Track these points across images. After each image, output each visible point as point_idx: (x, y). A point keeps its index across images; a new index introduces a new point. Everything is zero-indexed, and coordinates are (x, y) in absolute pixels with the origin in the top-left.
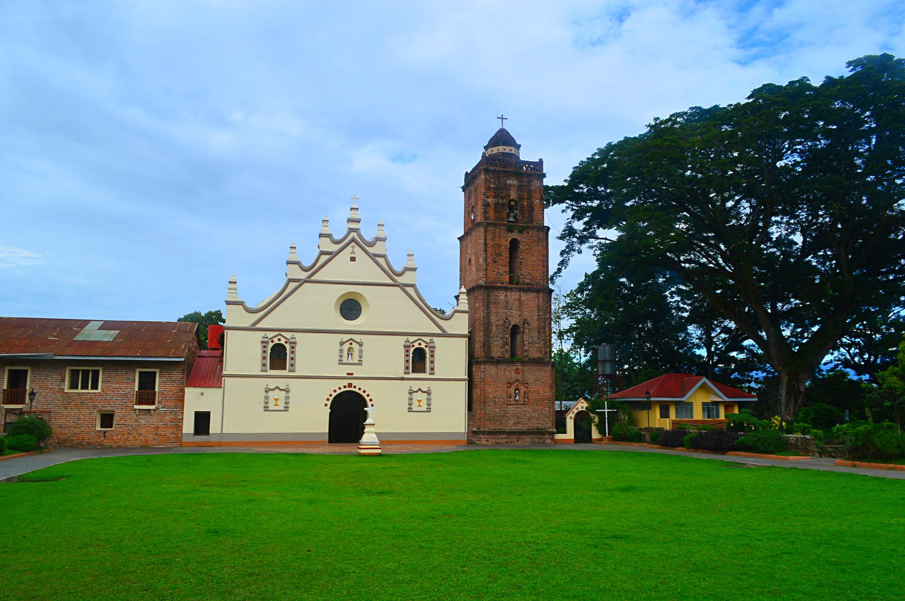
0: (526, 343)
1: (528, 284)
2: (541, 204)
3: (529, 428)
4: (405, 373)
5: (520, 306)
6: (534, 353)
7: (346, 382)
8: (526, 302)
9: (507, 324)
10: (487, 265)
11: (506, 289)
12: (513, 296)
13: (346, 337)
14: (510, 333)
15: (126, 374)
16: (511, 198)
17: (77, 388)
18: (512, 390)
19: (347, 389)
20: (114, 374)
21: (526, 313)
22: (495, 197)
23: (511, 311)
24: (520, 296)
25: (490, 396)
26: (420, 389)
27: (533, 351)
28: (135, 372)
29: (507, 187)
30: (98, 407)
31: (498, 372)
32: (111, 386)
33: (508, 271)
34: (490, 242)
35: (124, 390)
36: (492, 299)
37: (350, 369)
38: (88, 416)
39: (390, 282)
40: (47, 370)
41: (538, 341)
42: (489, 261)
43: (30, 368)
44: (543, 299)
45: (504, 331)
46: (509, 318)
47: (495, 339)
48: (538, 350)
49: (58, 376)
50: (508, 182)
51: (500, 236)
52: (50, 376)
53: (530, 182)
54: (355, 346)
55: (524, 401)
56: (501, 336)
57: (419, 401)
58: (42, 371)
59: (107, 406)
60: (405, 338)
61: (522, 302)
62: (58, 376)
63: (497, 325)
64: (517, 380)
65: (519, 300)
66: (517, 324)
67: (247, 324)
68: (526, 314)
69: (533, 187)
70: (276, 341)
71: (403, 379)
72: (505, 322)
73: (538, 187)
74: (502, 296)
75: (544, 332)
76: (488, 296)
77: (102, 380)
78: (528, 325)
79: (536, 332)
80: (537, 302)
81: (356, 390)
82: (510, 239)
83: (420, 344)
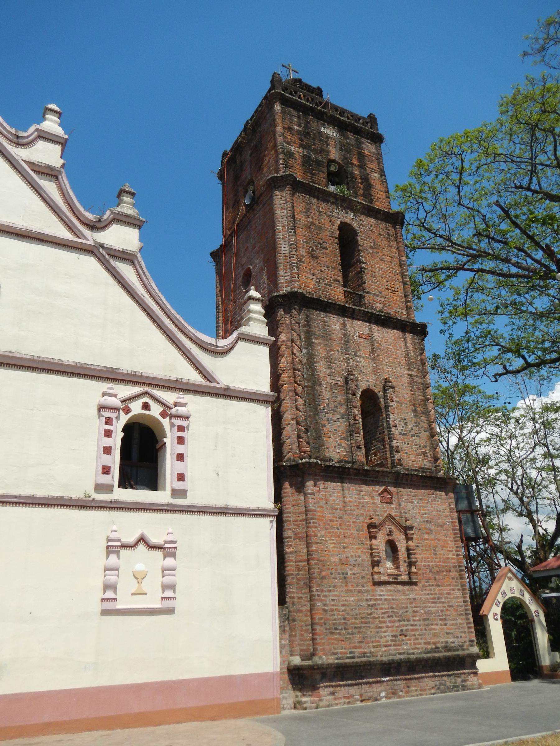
0: (395, 432)
2: (382, 181)
3: (429, 647)
4: (99, 488)
5: (373, 351)
6: (412, 458)
8: (383, 346)
9: (352, 384)
10: (300, 260)
14: (359, 406)
16: (332, 156)
18: (380, 543)
21: (385, 367)
22: (301, 146)
23: (357, 358)
24: (370, 330)
25: (333, 559)
26: (142, 539)
27: (410, 453)
31: (344, 497)
33: (340, 279)
34: (301, 218)
41: (415, 431)
44: (414, 344)
45: (348, 400)
46: (354, 372)
47: (329, 415)
48: (419, 451)
50: (322, 129)
51: (320, 212)
53: (359, 145)
55: (410, 574)
56: (342, 411)
57: (139, 577)
60: (105, 386)
61: (376, 344)
63: (331, 384)
64: (390, 517)
65: (369, 338)
66: (373, 388)
68: (387, 371)
69: (366, 152)
72: (347, 381)
73: (373, 153)
75: (426, 413)
78: (394, 392)
79: (410, 409)
80: (403, 348)
82: (339, 222)
83: (146, 406)
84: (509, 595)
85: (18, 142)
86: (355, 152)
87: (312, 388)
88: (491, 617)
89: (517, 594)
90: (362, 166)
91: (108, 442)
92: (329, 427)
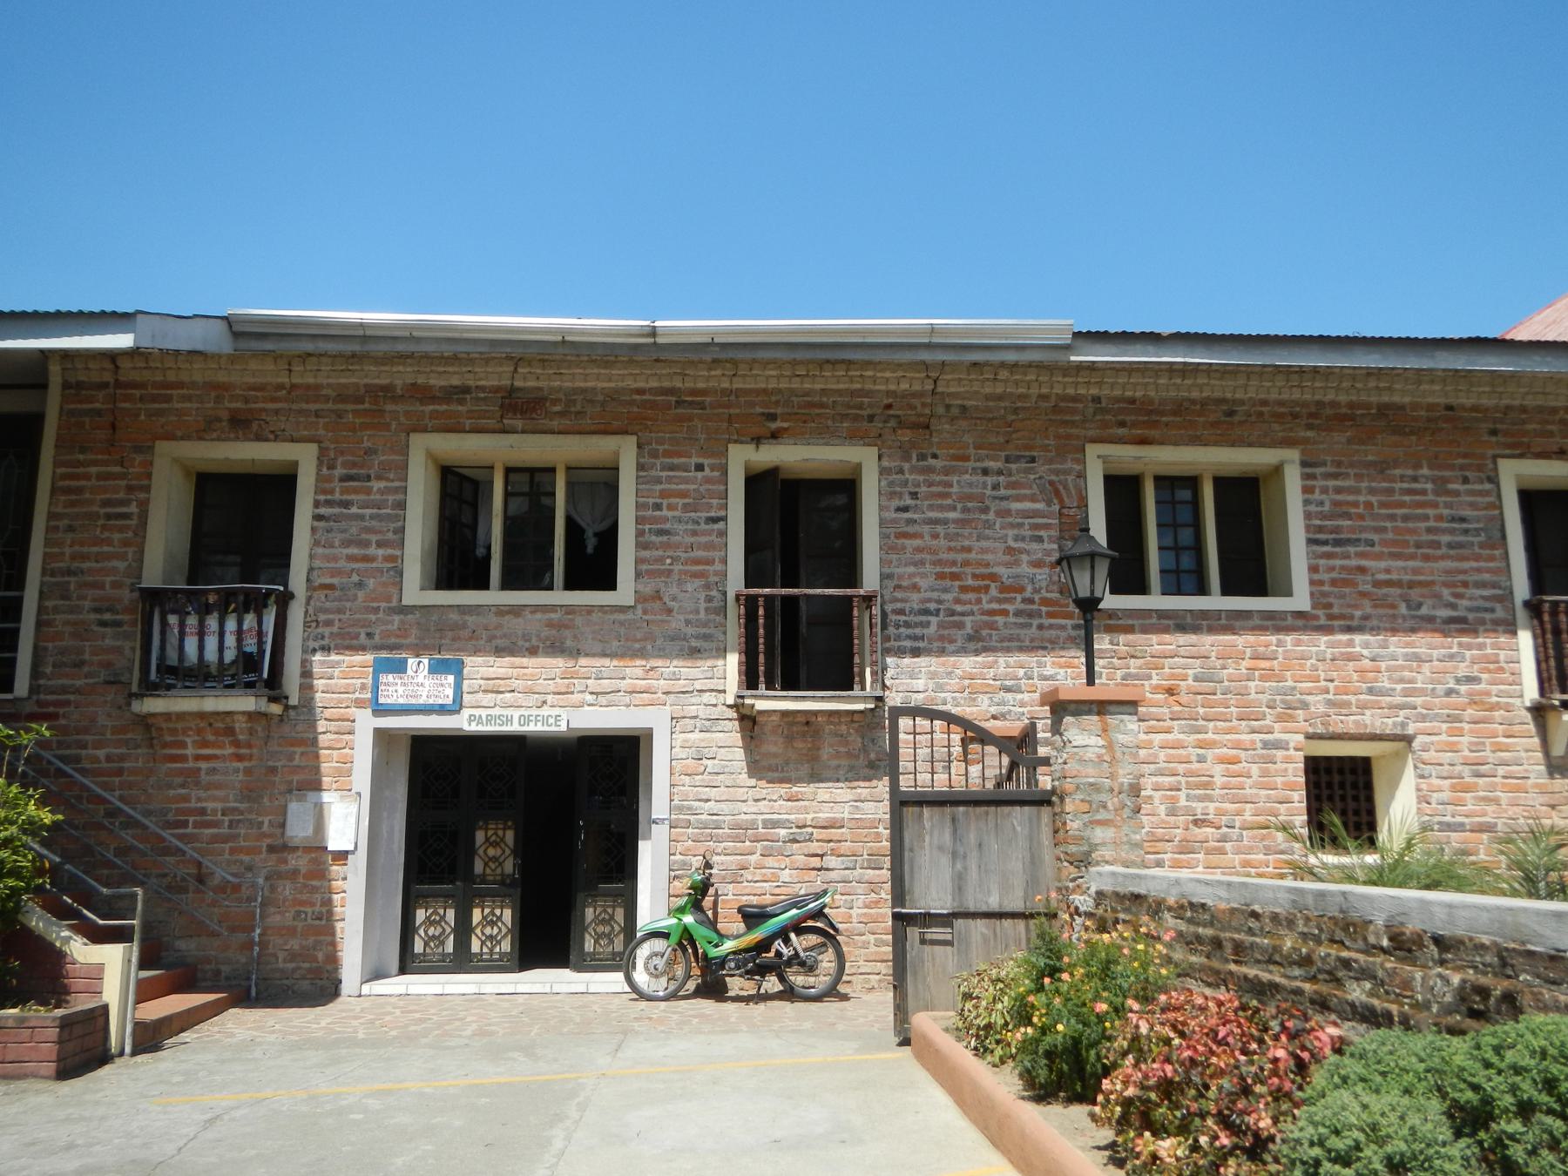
15: (1437, 493)
17: (1142, 588)
20: (1372, 491)
28: (1494, 480)
30: (1305, 706)
32: (1362, 570)
35: (1446, 592)
38: (1255, 770)
40: (971, 464)
43: (873, 452)
49: (1040, 506)
52: (994, 505)
58: (947, 471)
59: (1363, 707)
62: (1040, 506)
77: (1308, 528)
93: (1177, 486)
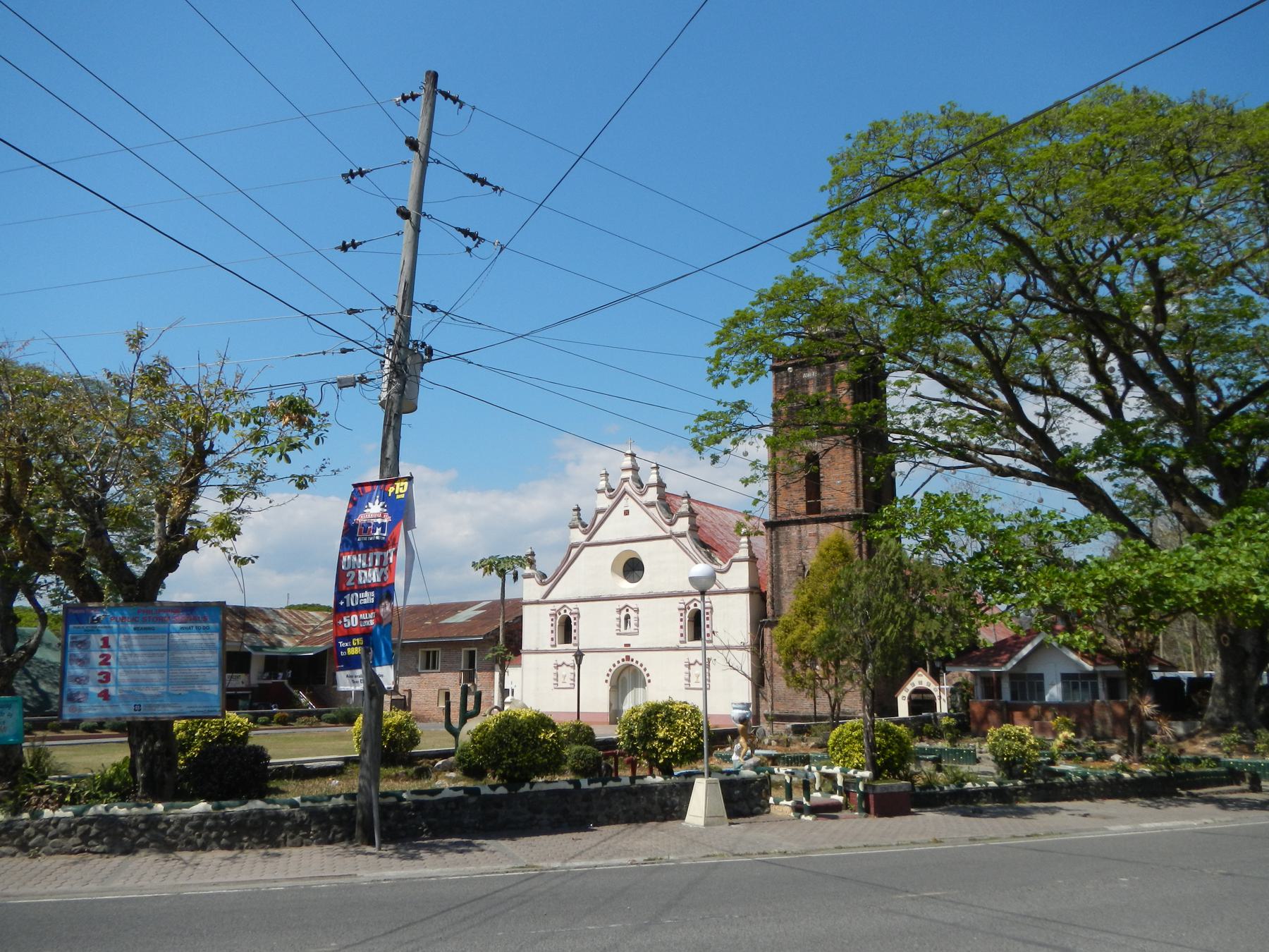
1: (832, 510)
4: (681, 642)
7: (623, 655)
11: (798, 522)
12: (810, 529)
13: (623, 603)
19: (626, 662)
24: (818, 529)
29: (804, 384)
33: (804, 496)
36: (782, 540)
37: (627, 640)
39: (662, 534)
42: (779, 486)
46: (804, 561)
50: (805, 376)
54: (631, 613)
60: (679, 599)
65: (817, 535)
67: (538, 597)
70: (562, 613)
71: (677, 649)
74: (793, 531)
76: (777, 535)
81: (634, 663)
83: (695, 605)
84: (917, 686)
85: (642, 495)
86: (829, 378)
87: (778, 576)
88: (899, 699)
89: (924, 685)
90: (833, 391)
91: (682, 623)
92: (787, 597)
93: (434, 652)
